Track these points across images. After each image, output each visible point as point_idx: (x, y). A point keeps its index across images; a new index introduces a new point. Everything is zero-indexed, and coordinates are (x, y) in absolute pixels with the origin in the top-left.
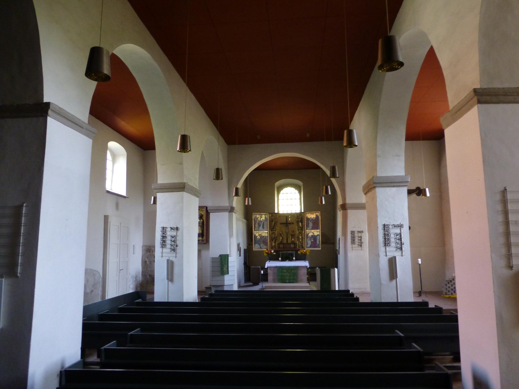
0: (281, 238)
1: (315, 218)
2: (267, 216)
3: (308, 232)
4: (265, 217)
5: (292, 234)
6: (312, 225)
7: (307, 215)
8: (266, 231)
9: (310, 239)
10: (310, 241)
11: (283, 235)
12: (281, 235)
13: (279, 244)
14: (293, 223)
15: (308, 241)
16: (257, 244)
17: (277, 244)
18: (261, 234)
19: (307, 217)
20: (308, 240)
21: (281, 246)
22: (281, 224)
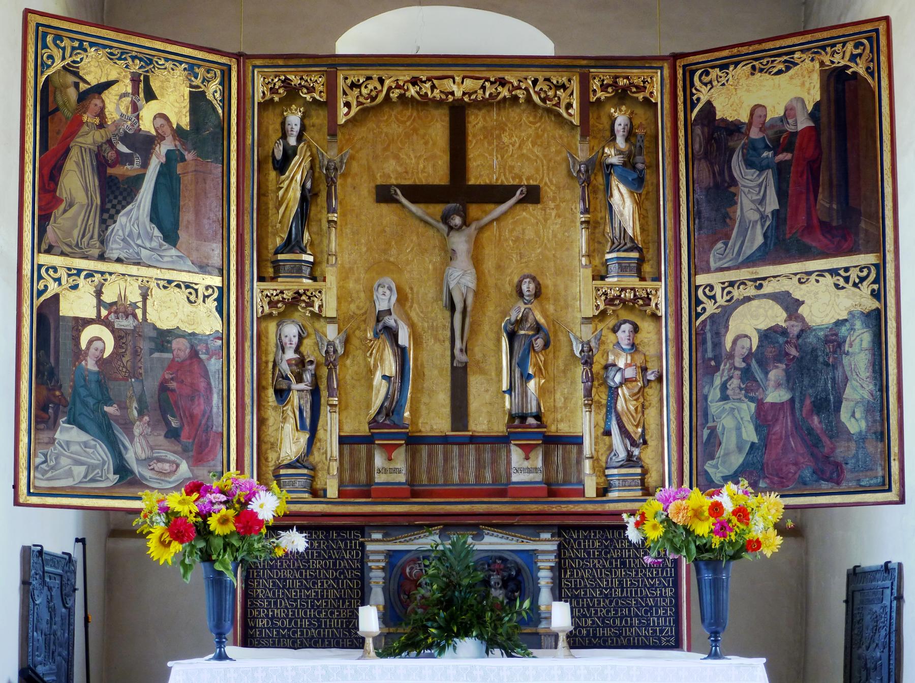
0: (390, 366)
1: (813, 115)
2: (213, 90)
3: (721, 301)
4: (197, 99)
5: (520, 322)
6: (772, 204)
7: (704, 94)
8: (203, 268)
9: (747, 374)
10: (748, 409)
11: (416, 337)
12: (392, 334)
13: (368, 440)
14: (533, 195)
15: (715, 407)
16: (72, 421)
17: (334, 448)
18: (134, 296)
19: (709, 108)
20: (725, 397)
21: (379, 461)
22: (384, 195)
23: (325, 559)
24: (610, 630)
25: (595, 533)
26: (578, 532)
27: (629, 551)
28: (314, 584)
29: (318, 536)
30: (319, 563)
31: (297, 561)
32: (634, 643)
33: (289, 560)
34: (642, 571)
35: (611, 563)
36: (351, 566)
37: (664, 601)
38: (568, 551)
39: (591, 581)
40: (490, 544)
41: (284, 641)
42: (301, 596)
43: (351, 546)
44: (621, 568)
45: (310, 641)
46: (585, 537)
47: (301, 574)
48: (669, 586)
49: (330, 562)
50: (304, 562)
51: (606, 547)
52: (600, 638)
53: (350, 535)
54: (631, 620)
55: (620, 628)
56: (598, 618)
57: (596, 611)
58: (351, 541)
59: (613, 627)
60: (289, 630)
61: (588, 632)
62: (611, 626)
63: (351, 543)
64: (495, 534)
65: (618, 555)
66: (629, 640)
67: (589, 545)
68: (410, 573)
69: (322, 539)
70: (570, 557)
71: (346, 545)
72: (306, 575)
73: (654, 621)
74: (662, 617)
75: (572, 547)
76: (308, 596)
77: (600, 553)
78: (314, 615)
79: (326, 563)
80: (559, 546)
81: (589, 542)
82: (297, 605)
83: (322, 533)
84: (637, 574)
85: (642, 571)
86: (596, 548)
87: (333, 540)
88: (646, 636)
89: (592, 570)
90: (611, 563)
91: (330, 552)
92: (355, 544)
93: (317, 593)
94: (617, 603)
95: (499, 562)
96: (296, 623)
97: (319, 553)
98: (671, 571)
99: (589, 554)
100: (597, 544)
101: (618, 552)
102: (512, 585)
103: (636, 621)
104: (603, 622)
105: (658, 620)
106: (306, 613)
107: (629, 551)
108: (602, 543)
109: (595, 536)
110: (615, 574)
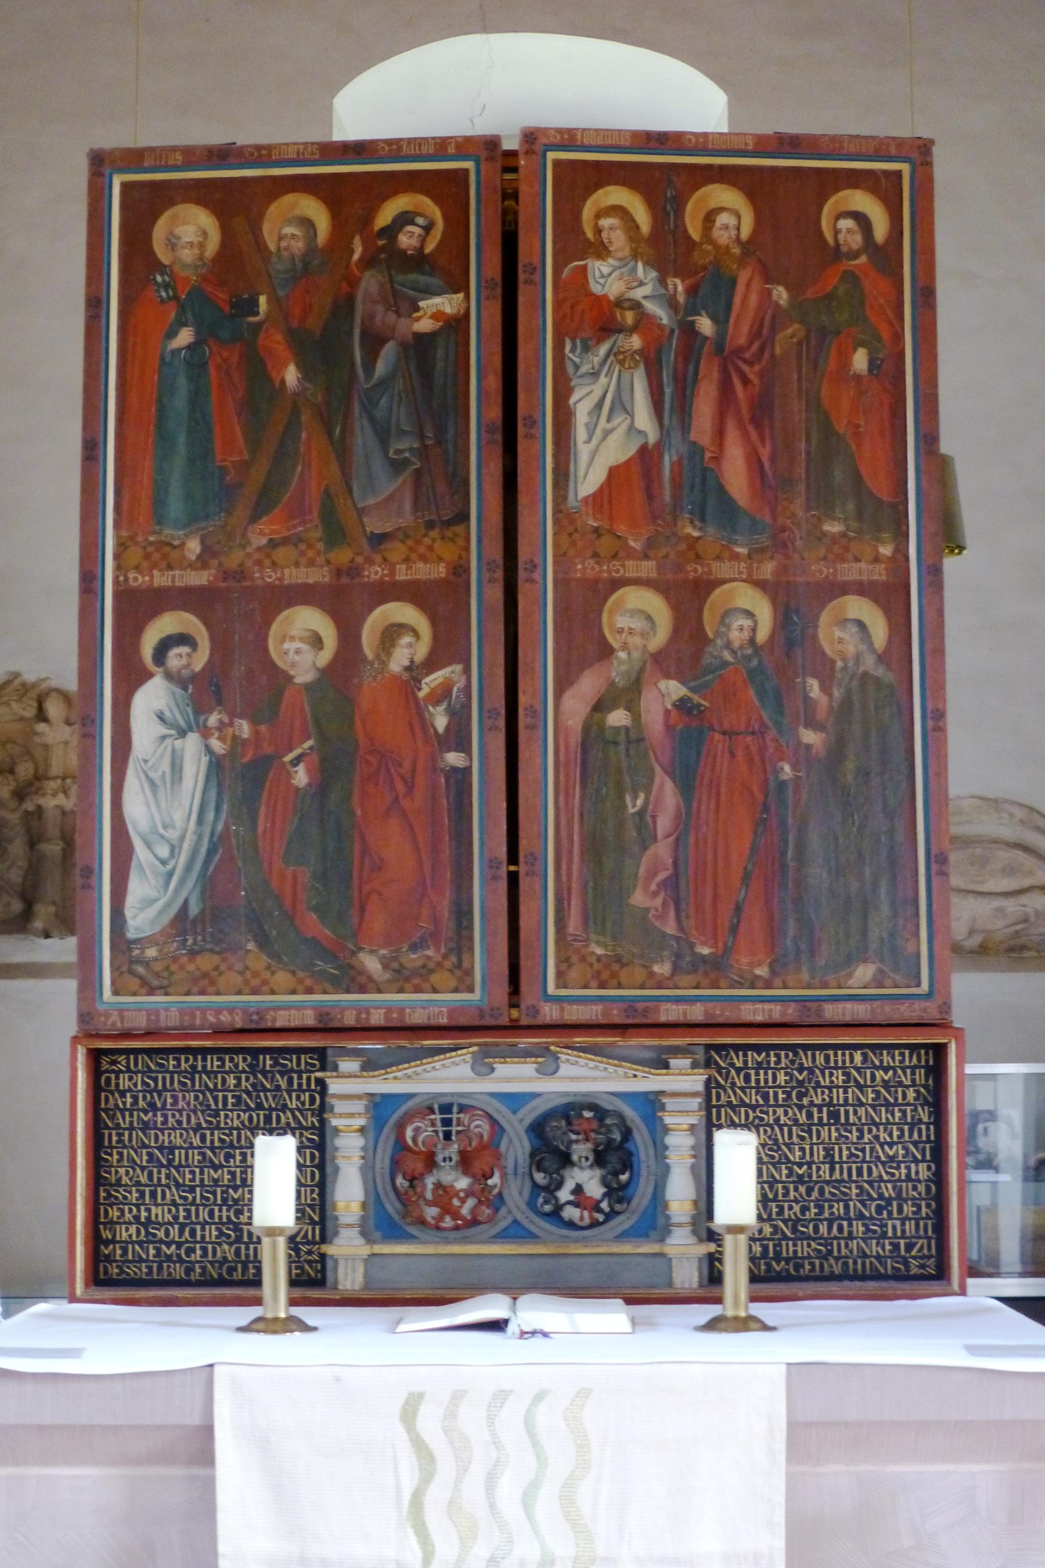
23: (249, 1109)
24: (809, 1246)
25: (778, 1056)
26: (745, 1055)
27: (845, 1092)
28: (228, 1157)
29: (236, 1066)
30: (239, 1116)
31: (195, 1114)
32: (855, 1270)
33: (180, 1111)
34: (870, 1131)
35: (810, 1116)
36: (299, 1122)
37: (915, 1188)
38: (725, 1091)
39: (770, 1150)
40: (572, 1079)
41: (169, 1267)
42: (202, 1180)
43: (300, 1085)
44: (829, 1124)
45: (221, 1268)
46: (759, 1065)
47: (203, 1139)
48: (924, 1160)
49: (258, 1115)
50: (210, 1115)
51: (801, 1083)
52: (788, 1260)
53: (299, 1064)
54: (850, 1225)
55: (827, 1242)
56: (785, 1221)
57: (781, 1209)
58: (300, 1073)
59: (814, 1239)
60: (179, 1245)
61: (765, 1248)
62: (809, 1238)
63: (300, 1078)
64: (582, 1061)
65: (824, 1100)
66: (846, 1264)
67: (766, 1081)
68: (415, 1139)
69: (244, 1071)
70: (730, 1104)
71: (290, 1082)
72: (212, 1141)
73: (894, 1228)
74: (910, 1219)
75: (733, 1084)
76: (216, 1181)
77: (789, 1095)
78: (228, 1217)
79: (251, 1119)
80: (708, 1083)
81: (766, 1074)
82: (194, 1198)
83: (245, 1060)
84: (861, 1137)
85: (870, 1131)
86: (780, 1087)
87: (264, 1073)
88: (878, 1257)
89: (773, 1129)
90: (810, 1116)
91: (258, 1097)
92: (309, 1079)
93: (233, 1174)
94: (822, 1192)
95: (587, 1114)
96: (193, 1233)
97: (238, 1098)
98: (928, 1129)
99: (765, 1097)
100: (782, 1078)
101: (823, 1093)
102: (614, 1160)
103: (859, 1228)
104: (794, 1230)
105: (903, 1224)
106: (211, 1214)
107: (845, 1092)
108: (792, 1076)
109: (778, 1062)
110: (819, 1137)
